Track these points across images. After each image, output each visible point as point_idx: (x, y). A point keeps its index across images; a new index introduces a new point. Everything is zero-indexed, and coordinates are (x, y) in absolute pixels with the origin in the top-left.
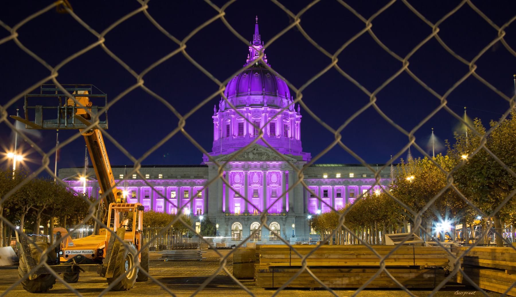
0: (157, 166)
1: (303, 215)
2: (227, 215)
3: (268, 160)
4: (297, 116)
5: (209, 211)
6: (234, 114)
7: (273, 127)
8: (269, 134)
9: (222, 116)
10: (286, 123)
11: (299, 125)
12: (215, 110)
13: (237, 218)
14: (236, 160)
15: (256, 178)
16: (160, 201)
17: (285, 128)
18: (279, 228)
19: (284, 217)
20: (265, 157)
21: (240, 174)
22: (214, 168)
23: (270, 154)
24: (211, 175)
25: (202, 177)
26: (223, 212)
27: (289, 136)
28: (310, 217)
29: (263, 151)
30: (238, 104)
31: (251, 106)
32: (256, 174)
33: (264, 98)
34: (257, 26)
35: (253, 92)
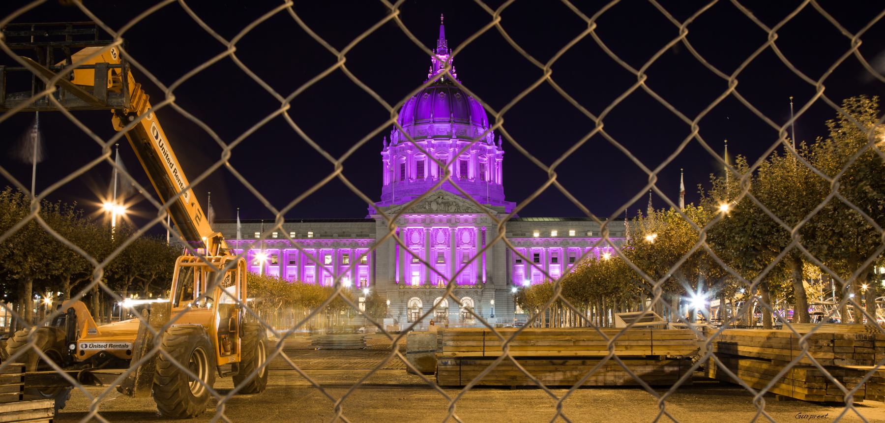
0: (304, 221)
1: (505, 288)
3: (458, 212)
4: (498, 152)
6: (411, 148)
7: (464, 166)
8: (458, 176)
9: (394, 152)
11: (500, 165)
12: (385, 143)
13: (416, 292)
14: (414, 213)
15: (441, 236)
16: (309, 269)
17: (481, 167)
18: (473, 306)
19: (480, 290)
20: (453, 209)
21: (420, 231)
22: (383, 223)
23: (461, 204)
24: (380, 232)
25: (367, 236)
27: (487, 179)
28: (514, 290)
29: (451, 199)
30: (416, 136)
31: (434, 137)
32: (441, 233)
33: (452, 127)
34: (442, 28)
35: (437, 119)
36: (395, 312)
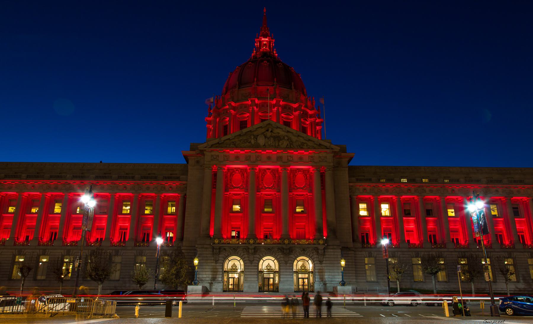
2: (216, 241)
5: (185, 236)
10: (305, 124)
19: (321, 247)
23: (294, 139)
26: (209, 236)
29: (282, 133)
36: (205, 275)
